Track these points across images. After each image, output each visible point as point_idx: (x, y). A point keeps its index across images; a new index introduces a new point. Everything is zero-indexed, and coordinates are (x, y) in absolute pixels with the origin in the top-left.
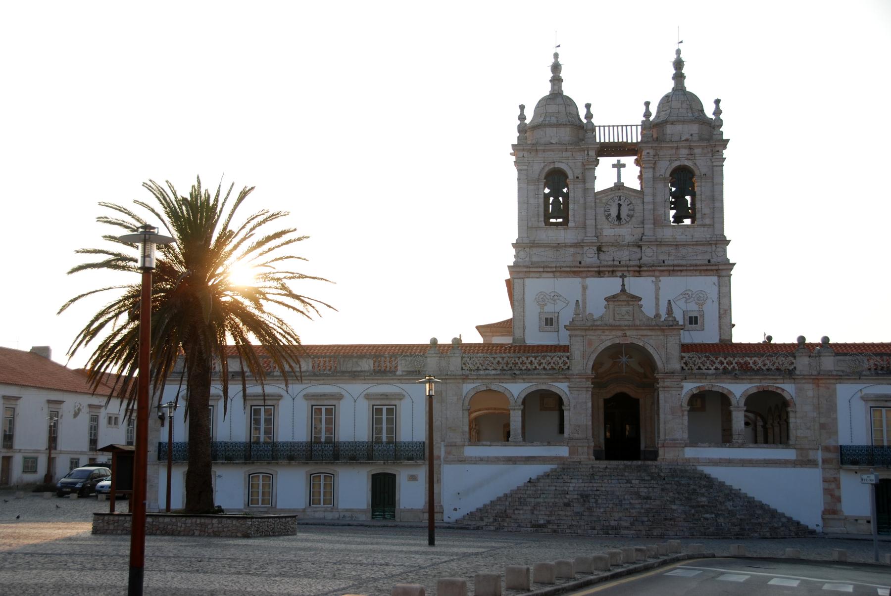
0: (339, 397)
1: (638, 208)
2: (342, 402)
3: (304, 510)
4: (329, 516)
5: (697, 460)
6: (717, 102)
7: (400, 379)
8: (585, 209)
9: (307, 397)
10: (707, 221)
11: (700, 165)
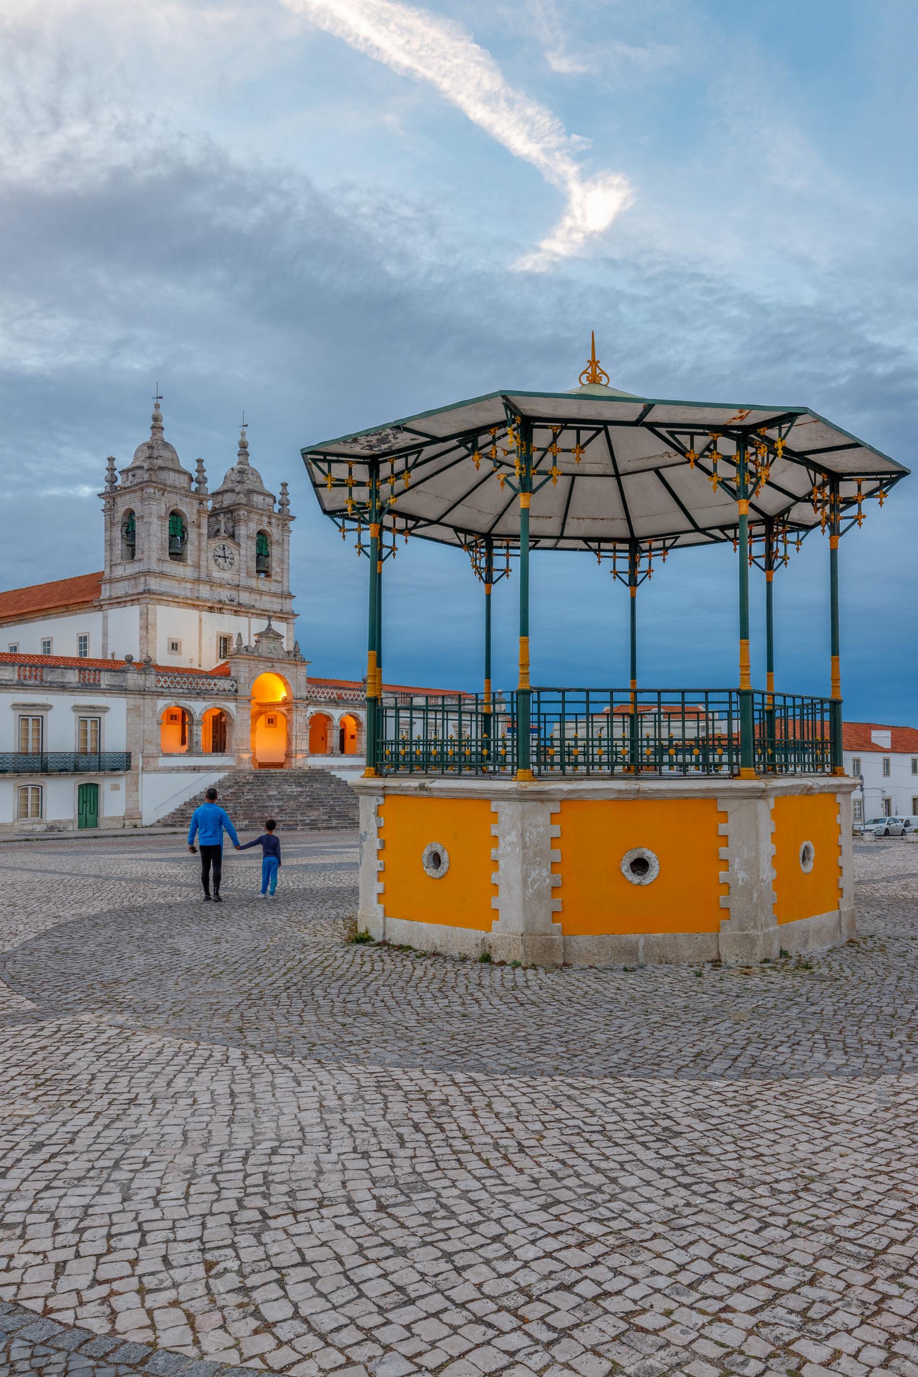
0: (47, 707)
1: (237, 558)
2: (50, 713)
3: (12, 825)
4: (39, 828)
5: (332, 767)
7: (104, 692)
8: (200, 550)
10: (279, 578)
11: (275, 532)
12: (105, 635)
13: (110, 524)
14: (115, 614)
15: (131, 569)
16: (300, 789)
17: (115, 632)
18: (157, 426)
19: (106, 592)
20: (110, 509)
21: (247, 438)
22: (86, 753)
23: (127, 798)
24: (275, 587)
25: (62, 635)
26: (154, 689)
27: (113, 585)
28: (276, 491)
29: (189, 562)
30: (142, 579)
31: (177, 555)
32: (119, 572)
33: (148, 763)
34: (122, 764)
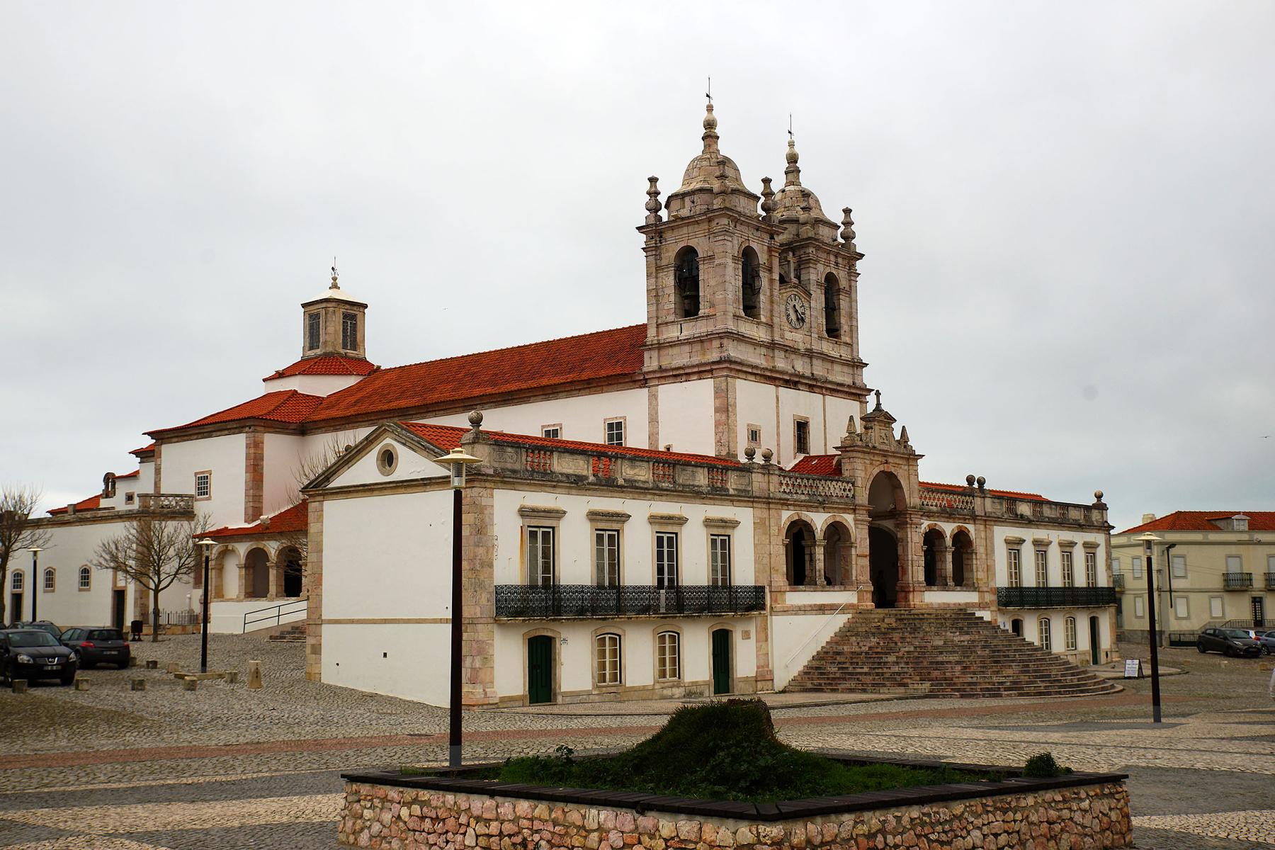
0: (682, 521)
6: (847, 212)
8: (772, 302)
9: (654, 520)
10: (849, 341)
11: (841, 275)
12: (654, 420)
13: (655, 270)
14: (669, 392)
15: (690, 329)
16: (967, 637)
17: (680, 417)
18: (710, 136)
19: (651, 362)
20: (657, 248)
21: (797, 149)
22: (717, 587)
23: (758, 649)
24: (844, 353)
25: (582, 418)
26: (779, 495)
27: (663, 352)
28: (838, 218)
29: (763, 319)
30: (716, 343)
31: (750, 309)
32: (672, 333)
33: (776, 601)
34: (753, 602)
